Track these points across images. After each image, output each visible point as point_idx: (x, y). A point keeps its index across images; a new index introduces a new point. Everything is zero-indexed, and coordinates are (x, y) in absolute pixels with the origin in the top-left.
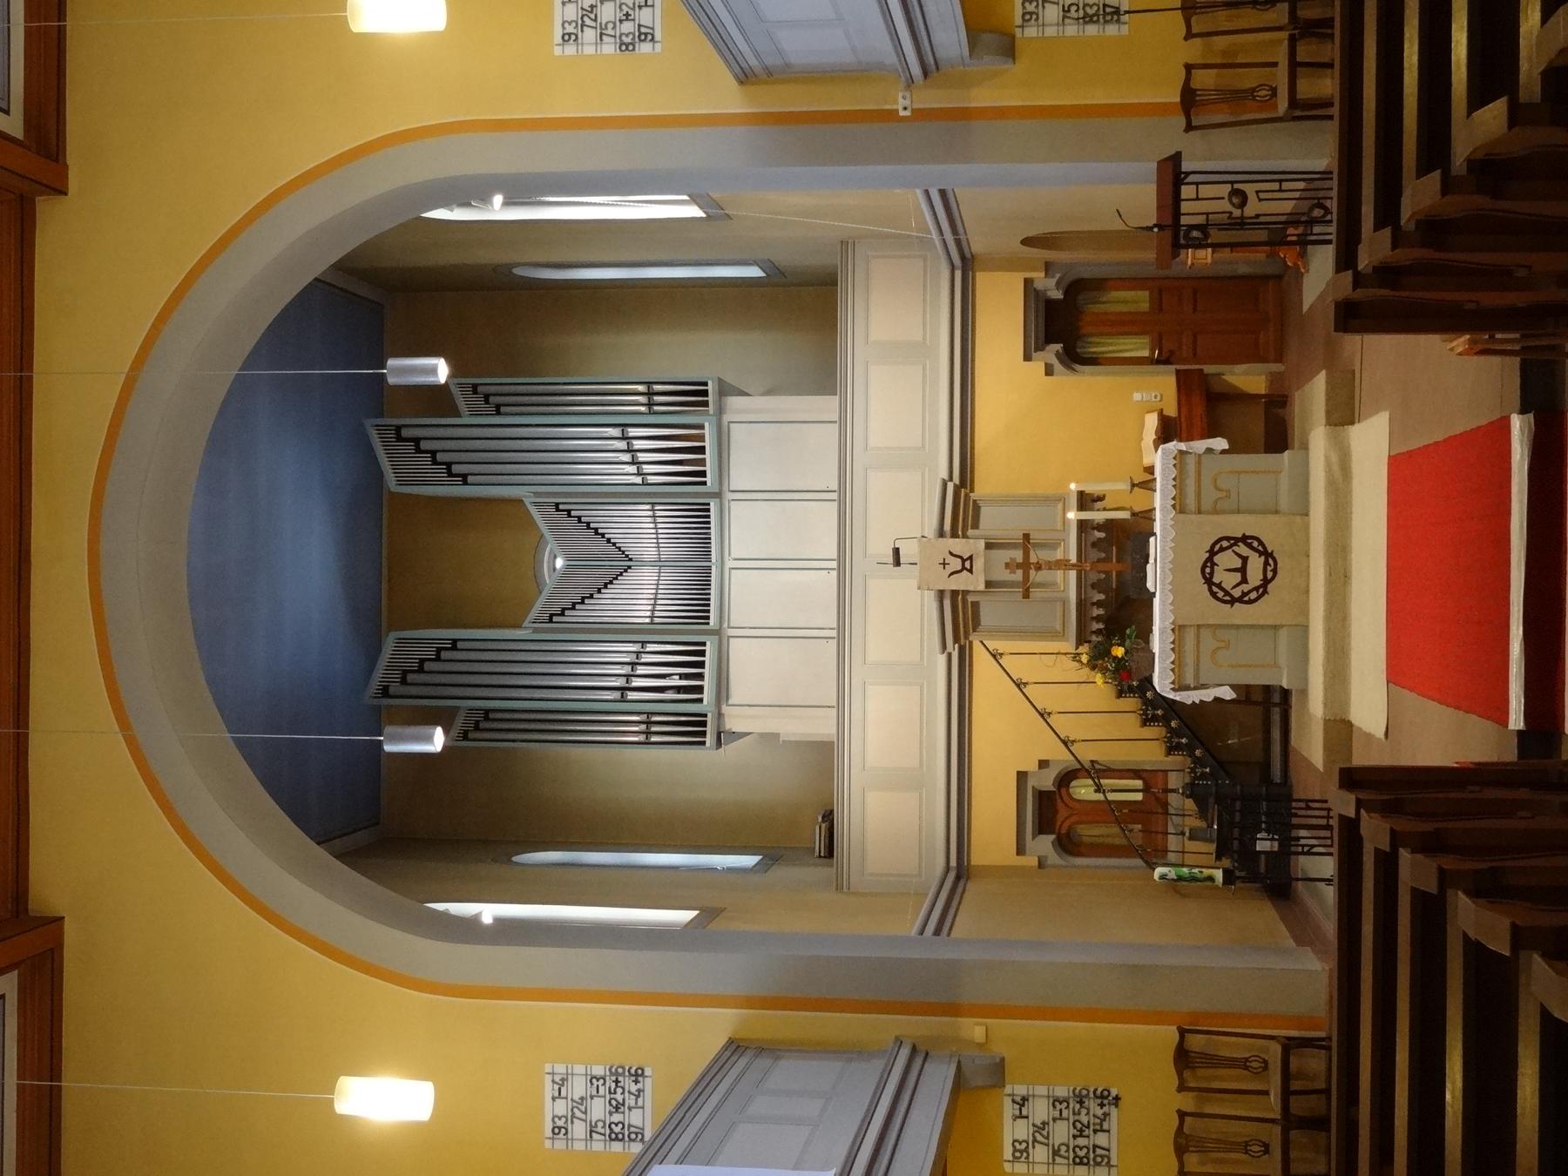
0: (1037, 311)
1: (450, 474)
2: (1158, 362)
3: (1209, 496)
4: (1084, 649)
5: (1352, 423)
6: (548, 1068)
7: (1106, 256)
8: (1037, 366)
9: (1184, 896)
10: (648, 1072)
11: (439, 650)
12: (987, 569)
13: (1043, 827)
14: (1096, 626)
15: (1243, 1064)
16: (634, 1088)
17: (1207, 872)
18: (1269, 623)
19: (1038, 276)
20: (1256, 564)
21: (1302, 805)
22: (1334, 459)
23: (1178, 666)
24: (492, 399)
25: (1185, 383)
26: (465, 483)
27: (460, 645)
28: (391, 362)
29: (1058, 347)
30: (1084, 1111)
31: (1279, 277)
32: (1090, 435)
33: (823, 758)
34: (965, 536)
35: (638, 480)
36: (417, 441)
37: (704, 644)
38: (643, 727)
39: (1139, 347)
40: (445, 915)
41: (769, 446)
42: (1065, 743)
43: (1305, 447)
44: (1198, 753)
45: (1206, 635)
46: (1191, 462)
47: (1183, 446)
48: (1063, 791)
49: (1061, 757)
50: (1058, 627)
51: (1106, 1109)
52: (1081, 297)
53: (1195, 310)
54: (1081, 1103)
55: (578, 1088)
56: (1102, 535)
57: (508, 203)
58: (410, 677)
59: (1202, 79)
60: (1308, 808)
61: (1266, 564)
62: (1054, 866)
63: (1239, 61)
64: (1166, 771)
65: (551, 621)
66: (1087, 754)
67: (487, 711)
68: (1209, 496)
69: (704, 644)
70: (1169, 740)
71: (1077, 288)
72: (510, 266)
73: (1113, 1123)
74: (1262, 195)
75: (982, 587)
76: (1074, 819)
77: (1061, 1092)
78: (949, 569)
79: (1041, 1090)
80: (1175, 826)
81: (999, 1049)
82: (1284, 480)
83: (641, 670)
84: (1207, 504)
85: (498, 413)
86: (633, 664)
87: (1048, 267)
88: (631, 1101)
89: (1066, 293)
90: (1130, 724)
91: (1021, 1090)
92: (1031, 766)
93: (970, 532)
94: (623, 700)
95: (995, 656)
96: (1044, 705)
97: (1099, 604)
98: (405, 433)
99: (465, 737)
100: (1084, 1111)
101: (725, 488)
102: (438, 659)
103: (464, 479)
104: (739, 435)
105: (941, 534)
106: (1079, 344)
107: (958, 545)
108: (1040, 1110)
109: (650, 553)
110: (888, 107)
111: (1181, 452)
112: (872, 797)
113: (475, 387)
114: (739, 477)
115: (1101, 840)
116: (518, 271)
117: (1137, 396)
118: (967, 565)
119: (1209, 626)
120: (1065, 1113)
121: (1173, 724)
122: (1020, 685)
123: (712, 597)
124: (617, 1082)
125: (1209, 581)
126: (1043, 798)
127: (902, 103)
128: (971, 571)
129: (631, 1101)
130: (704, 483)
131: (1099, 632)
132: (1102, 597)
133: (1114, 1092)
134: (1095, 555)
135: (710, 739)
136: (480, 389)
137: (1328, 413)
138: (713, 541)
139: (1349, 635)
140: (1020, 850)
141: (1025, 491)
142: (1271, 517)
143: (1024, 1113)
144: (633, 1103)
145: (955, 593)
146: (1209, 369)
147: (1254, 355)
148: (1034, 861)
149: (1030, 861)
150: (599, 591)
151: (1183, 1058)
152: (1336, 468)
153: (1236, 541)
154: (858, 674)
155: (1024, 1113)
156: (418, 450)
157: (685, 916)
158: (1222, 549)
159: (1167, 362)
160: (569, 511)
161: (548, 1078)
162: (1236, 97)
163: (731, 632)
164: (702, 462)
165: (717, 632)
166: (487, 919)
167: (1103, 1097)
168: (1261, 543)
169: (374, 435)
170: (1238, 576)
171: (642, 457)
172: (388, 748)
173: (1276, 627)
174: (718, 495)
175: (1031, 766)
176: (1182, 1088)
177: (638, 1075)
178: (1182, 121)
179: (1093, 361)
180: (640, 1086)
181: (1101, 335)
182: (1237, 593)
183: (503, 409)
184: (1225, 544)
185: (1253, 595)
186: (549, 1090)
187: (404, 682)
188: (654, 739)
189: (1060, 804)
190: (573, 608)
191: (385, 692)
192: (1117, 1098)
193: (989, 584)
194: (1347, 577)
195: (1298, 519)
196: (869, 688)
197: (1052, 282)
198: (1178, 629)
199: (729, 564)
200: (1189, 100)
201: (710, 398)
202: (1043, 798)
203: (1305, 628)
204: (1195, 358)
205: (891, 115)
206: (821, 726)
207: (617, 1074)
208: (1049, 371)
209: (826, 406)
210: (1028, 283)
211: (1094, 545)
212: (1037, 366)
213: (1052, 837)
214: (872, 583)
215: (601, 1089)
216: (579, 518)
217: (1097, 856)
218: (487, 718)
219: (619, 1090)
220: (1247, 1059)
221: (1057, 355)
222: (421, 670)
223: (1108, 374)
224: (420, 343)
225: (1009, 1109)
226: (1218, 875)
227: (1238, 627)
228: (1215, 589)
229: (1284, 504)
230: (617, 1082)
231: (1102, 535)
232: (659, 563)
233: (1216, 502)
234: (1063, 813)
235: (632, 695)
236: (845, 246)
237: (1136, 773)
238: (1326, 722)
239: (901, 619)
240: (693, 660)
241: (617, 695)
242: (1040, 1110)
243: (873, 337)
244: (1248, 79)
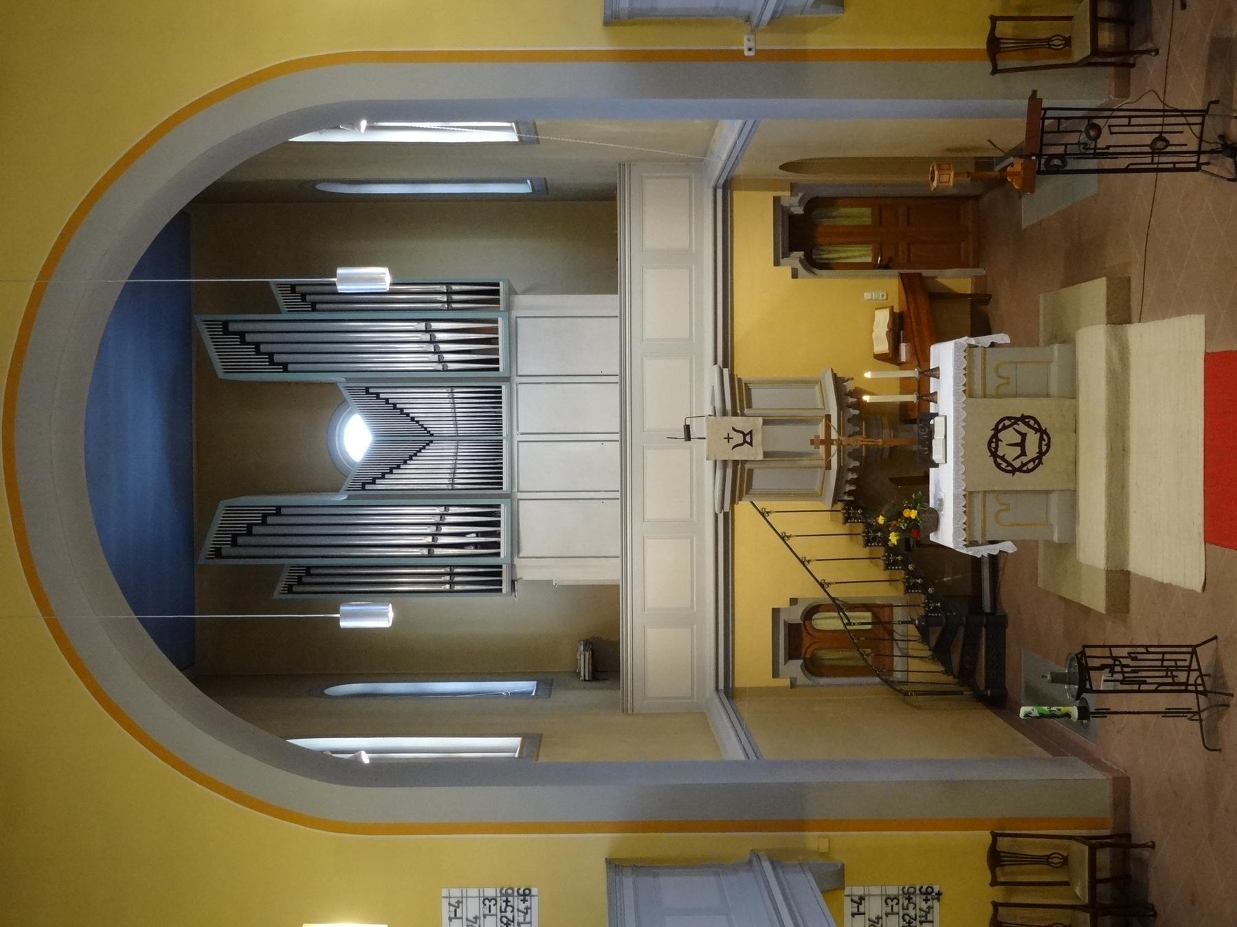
0: (783, 226)
1: (272, 362)
3: (993, 381)
4: (840, 506)
5: (1129, 322)
6: (445, 892)
7: (887, 179)
8: (785, 270)
9: (919, 708)
10: (534, 891)
11: (265, 516)
12: (763, 444)
13: (792, 654)
14: (848, 488)
15: (1046, 860)
16: (522, 906)
17: (1064, 709)
18: (1044, 488)
19: (785, 195)
20: (1033, 439)
21: (1143, 650)
22: (1115, 353)
23: (969, 527)
24: (308, 298)
25: (911, 285)
26: (286, 370)
27: (283, 511)
28: (340, 271)
30: (911, 906)
31: (977, 198)
32: (826, 328)
33: (605, 602)
34: (743, 415)
35: (440, 367)
36: (242, 334)
37: (498, 506)
38: (448, 578)
39: (862, 254)
40: (320, 755)
41: (551, 334)
42: (822, 585)
43: (1064, 337)
44: (930, 590)
45: (990, 497)
46: (978, 353)
47: (973, 341)
49: (814, 594)
50: (817, 489)
51: (930, 903)
52: (814, 213)
54: (909, 899)
55: (472, 908)
56: (857, 412)
57: (370, 128)
58: (240, 540)
59: (1004, 29)
60: (1148, 653)
61: (1041, 439)
62: (804, 686)
63: (1033, 14)
64: (891, 606)
65: (363, 488)
66: (833, 591)
67: (308, 569)
68: (993, 381)
69: (498, 506)
70: (908, 580)
71: (815, 204)
72: (315, 182)
73: (936, 915)
74: (1113, 129)
75: (760, 457)
76: (815, 646)
77: (893, 890)
78: (733, 443)
79: (875, 890)
80: (900, 649)
81: (839, 858)
82: (1054, 368)
83: (445, 529)
84: (991, 389)
85: (314, 309)
86: (438, 525)
87: (793, 187)
88: (520, 917)
89: (805, 209)
90: (877, 572)
91: (858, 891)
92: (783, 604)
93: (746, 411)
94: (430, 556)
95: (764, 514)
96: (801, 551)
97: (853, 470)
98: (232, 327)
99: (290, 590)
100: (911, 906)
101: (514, 373)
102: (264, 523)
103: (285, 367)
104: (525, 328)
105: (724, 413)
107: (740, 423)
108: (874, 907)
109: (447, 427)
110: (735, 48)
111: (971, 346)
112: (651, 633)
113: (293, 287)
114: (526, 364)
115: (838, 663)
116: (319, 187)
117: (867, 296)
118: (748, 439)
119: (994, 491)
120: (896, 909)
121: (910, 567)
122: (784, 538)
123: (504, 466)
124: (507, 901)
125: (994, 454)
126: (792, 629)
127: (746, 44)
128: (751, 444)
129: (520, 917)
130: (497, 369)
131: (850, 493)
132: (857, 464)
133: (936, 889)
134: (850, 428)
135: (505, 587)
136: (298, 289)
137: (1109, 314)
138: (504, 418)
139: (1127, 501)
140: (776, 674)
141: (792, 375)
142: (1045, 401)
143: (861, 910)
144: (521, 920)
145: (735, 463)
146: (926, 273)
147: (956, 262)
148: (787, 682)
149: (784, 682)
150: (405, 462)
151: (996, 858)
152: (1116, 359)
153: (1016, 420)
154: (638, 528)
155: (861, 910)
156: (243, 342)
157: (515, 742)
158: (1005, 428)
159: (884, 266)
160: (378, 394)
161: (445, 902)
162: (1028, 45)
163: (520, 496)
164: (496, 351)
165: (508, 496)
166: (365, 758)
167: (928, 894)
168: (1036, 422)
169: (203, 328)
170: (1018, 450)
171: (443, 347)
172: (344, 624)
173: (1047, 492)
174: (507, 379)
175: (783, 604)
176: (994, 883)
177: (525, 895)
178: (988, 66)
179: (826, 266)
180: (527, 904)
181: (830, 244)
182: (1017, 464)
183: (318, 306)
184: (1007, 423)
185: (1031, 466)
186: (446, 912)
187: (234, 544)
188: (457, 588)
189: (804, 634)
190: (383, 477)
191: (218, 553)
192: (939, 894)
193: (766, 454)
194: (1125, 451)
195: (1067, 402)
196: (648, 542)
197: (796, 200)
198: (969, 495)
199: (517, 438)
200: (994, 46)
201: (502, 297)
202: (792, 629)
203: (1074, 493)
204: (909, 263)
205: (737, 55)
206: (606, 573)
207: (507, 895)
208: (795, 275)
209: (606, 303)
210: (776, 200)
211: (849, 420)
212: (785, 270)
213: (800, 662)
214: (649, 454)
215: (493, 908)
216: (387, 400)
217: (835, 676)
218: (308, 574)
219: (509, 909)
220: (1048, 857)
221: (801, 261)
222: (249, 533)
224: (246, 249)
225: (849, 908)
226: (1074, 711)
227: (1017, 492)
228: (999, 461)
229: (1054, 389)
230: (507, 901)
231: (857, 412)
232: (457, 438)
233: (998, 387)
234: (807, 641)
235: (438, 551)
236: (621, 165)
238: (1109, 573)
239: (680, 485)
240: (489, 521)
241: (425, 551)
242: (874, 907)
243: (649, 243)
244: (1042, 31)
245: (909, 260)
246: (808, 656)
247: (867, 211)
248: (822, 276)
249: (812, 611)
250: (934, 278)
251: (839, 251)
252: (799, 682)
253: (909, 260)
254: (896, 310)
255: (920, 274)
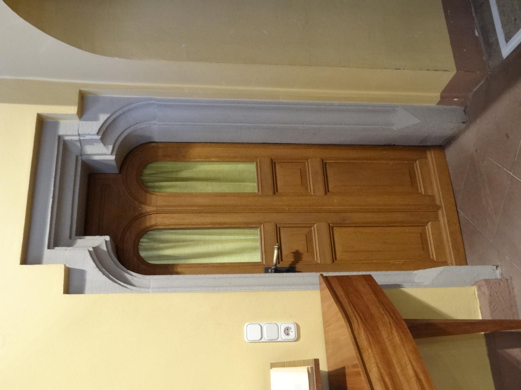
2: (277, 270)
25: (355, 300)
29: (101, 241)
31: (442, 145)
39: (244, 246)
52: (147, 171)
53: (327, 191)
87: (85, 103)
106: (144, 242)
117: (251, 332)
179: (167, 269)
197: (91, 128)
208: (73, 283)
210: (43, 124)
212: (50, 273)
221: (96, 254)
223: (190, 289)
245: (334, 258)
247: (249, 169)
248: (146, 288)
250: (398, 286)
251: (196, 243)
253: (334, 258)
254: (324, 367)
255: (369, 279)
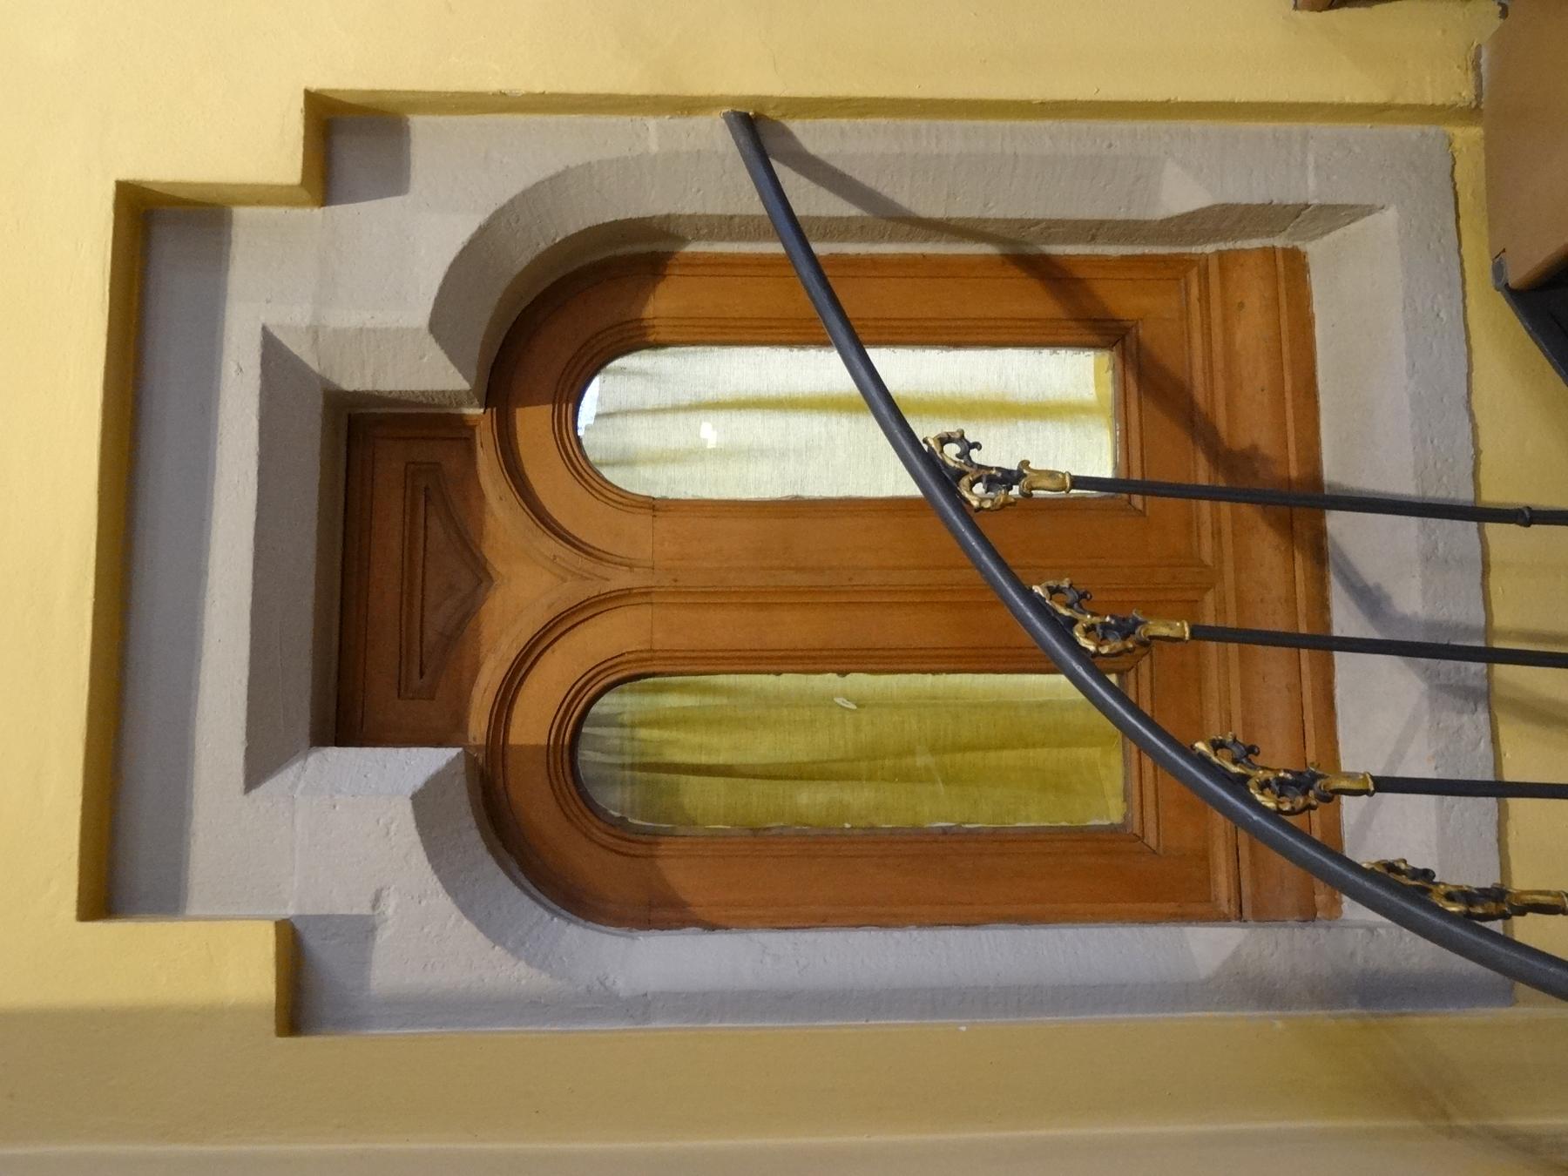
48: (532, 422)
115: (810, 800)
148: (246, 971)
149: (215, 960)
189: (500, 510)
213: (427, 761)
237: (1042, 286)
246: (532, 724)
249: (569, 302)
252: (392, 967)
